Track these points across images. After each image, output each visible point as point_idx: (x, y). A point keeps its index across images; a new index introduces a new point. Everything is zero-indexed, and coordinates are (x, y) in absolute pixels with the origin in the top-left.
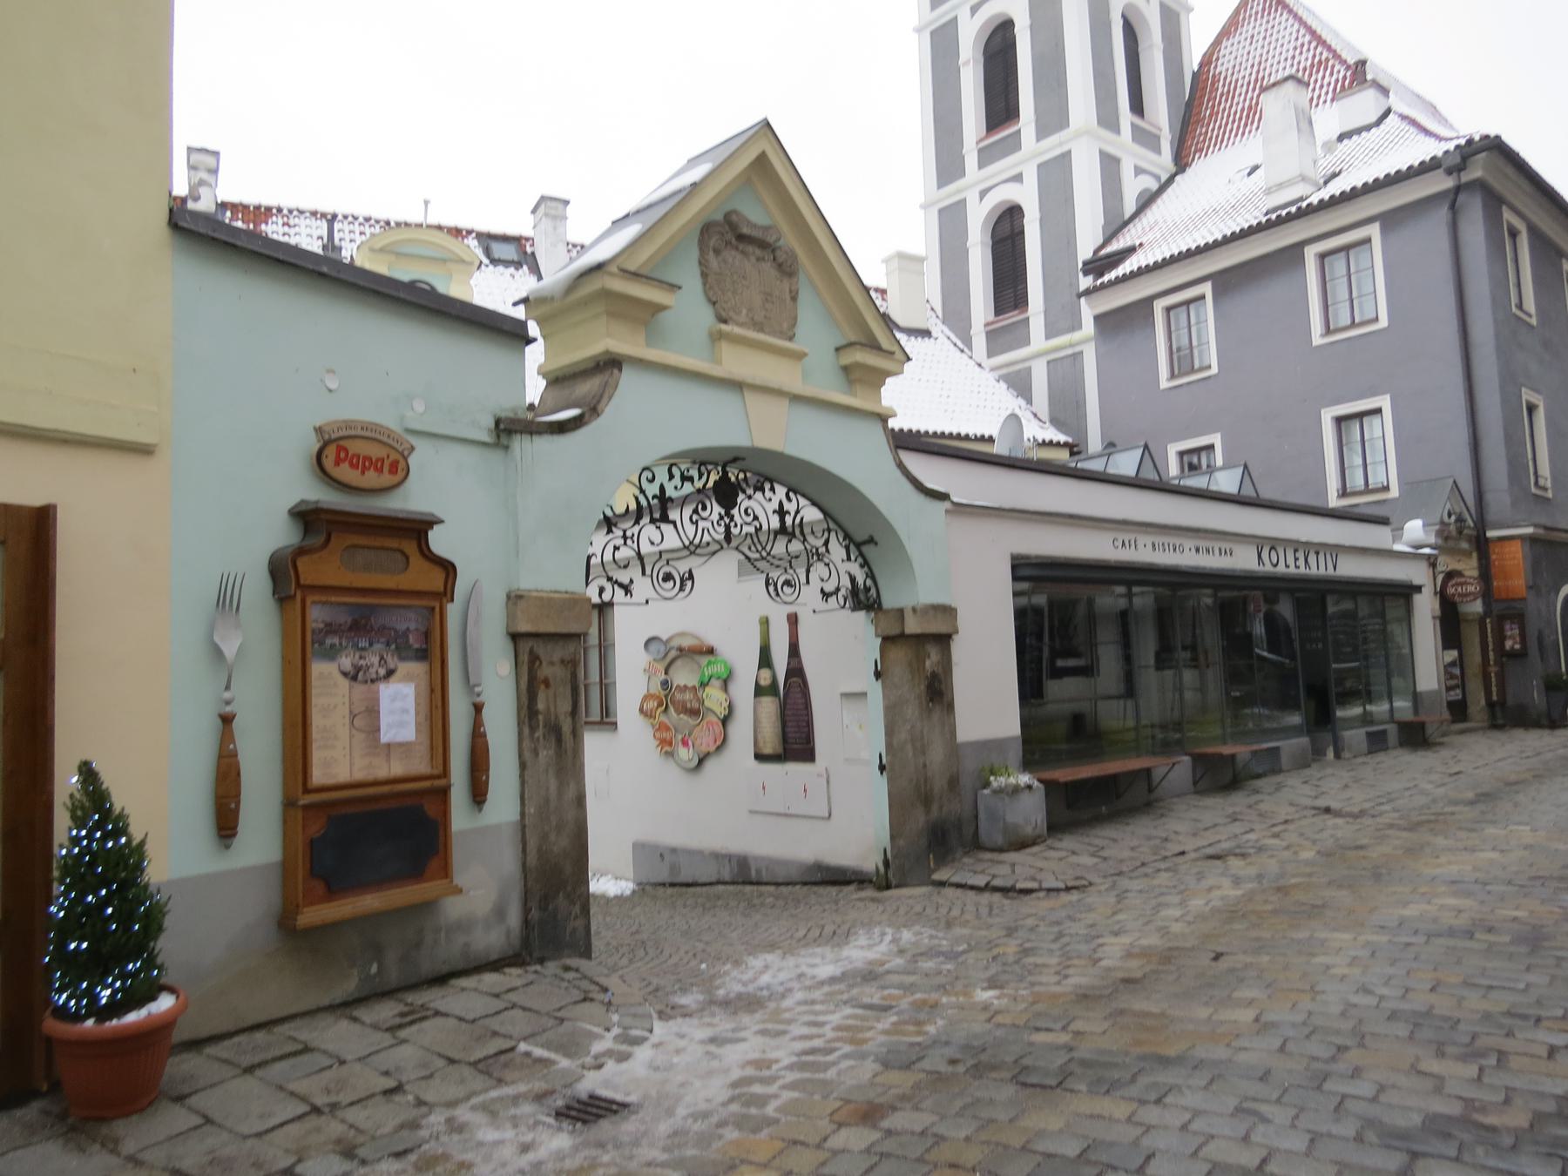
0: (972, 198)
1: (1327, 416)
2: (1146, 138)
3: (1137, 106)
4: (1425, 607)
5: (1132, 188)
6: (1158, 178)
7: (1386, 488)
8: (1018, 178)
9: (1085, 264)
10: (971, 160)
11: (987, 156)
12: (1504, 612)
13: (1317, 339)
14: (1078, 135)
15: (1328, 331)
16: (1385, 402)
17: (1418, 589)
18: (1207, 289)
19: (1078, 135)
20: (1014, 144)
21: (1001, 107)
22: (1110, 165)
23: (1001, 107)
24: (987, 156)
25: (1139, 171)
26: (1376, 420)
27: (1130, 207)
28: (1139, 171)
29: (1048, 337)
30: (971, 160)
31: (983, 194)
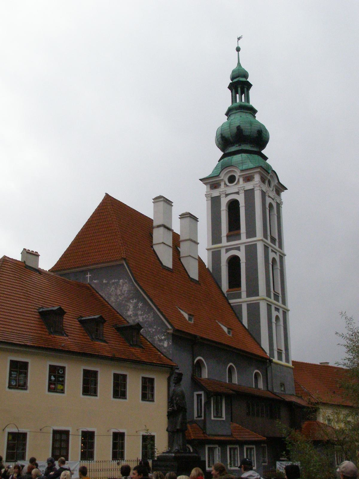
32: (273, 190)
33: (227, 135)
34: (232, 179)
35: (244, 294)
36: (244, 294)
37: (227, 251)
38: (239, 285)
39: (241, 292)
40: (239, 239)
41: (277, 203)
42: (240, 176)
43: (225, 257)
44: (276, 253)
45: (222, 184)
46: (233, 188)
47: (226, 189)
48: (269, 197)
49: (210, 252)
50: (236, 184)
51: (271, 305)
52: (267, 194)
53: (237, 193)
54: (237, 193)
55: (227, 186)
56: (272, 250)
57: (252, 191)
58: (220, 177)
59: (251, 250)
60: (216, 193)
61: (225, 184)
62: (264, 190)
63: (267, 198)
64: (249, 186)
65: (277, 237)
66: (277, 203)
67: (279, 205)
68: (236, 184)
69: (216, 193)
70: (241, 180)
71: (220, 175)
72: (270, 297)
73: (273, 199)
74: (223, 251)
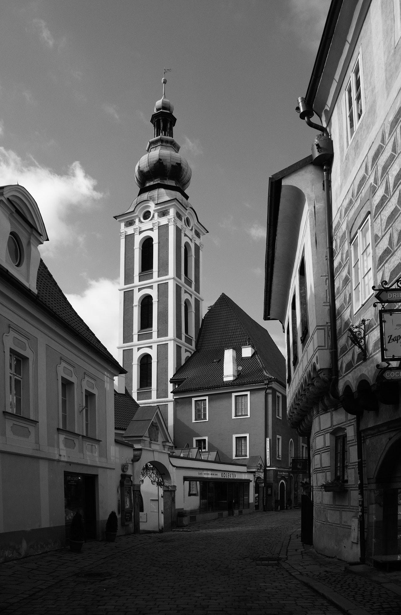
0: (135, 349)
1: (234, 436)
4: (252, 485)
5: (184, 355)
7: (246, 456)
8: (151, 347)
9: (171, 379)
10: (135, 337)
11: (140, 338)
12: (268, 485)
13: (234, 417)
15: (236, 416)
16: (247, 435)
17: (251, 481)
18: (207, 398)
19: (171, 340)
20: (150, 336)
21: (146, 322)
22: (178, 349)
23: (146, 322)
24: (140, 338)
25: (186, 351)
28: (186, 351)
30: (135, 337)
31: (139, 349)
33: (146, 170)
34: (147, 215)
35: (155, 334)
36: (155, 334)
37: (140, 290)
38: (150, 325)
40: (152, 278)
42: (154, 211)
43: (137, 297)
45: (137, 220)
46: (147, 224)
47: (141, 225)
48: (186, 235)
49: (123, 292)
50: (151, 220)
51: (181, 347)
52: (183, 231)
53: (152, 229)
54: (152, 229)
55: (142, 222)
57: (167, 226)
59: (163, 289)
60: (130, 230)
61: (140, 221)
62: (180, 227)
63: (183, 235)
68: (151, 220)
69: (130, 230)
71: (135, 211)
72: (181, 338)
74: (136, 290)
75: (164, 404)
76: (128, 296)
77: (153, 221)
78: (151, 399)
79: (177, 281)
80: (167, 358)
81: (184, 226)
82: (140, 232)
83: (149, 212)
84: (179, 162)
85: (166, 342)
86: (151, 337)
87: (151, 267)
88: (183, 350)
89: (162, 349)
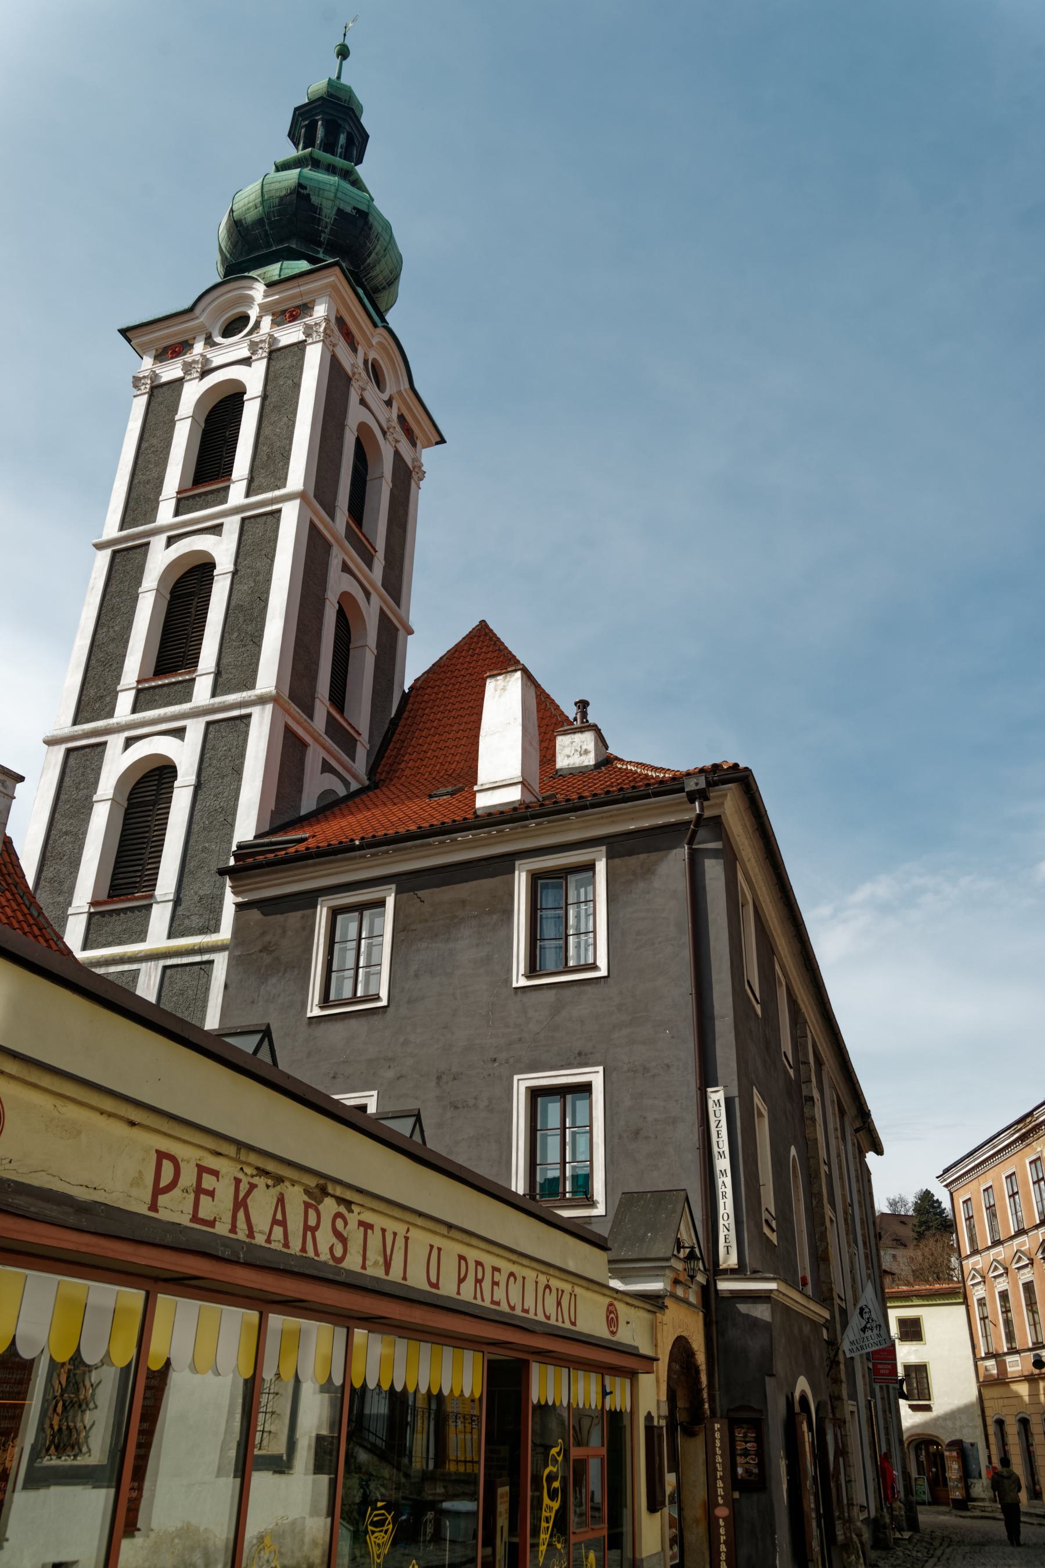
1: (522, 1084)
2: (341, 735)
3: (338, 697)
5: (315, 785)
6: (346, 784)
8: (179, 733)
9: (240, 847)
10: (125, 701)
14: (262, 700)
16: (596, 1077)
19: (262, 700)
21: (174, 650)
25: (326, 768)
26: (581, 1105)
27: (308, 804)
28: (326, 768)
29: (170, 936)
30: (125, 701)
31: (129, 742)
32: (389, 403)
33: (251, 216)
34: (235, 325)
39: (194, 680)
41: (397, 454)
44: (368, 595)
53: (246, 362)
55: (215, 344)
56: (344, 563)
58: (197, 318)
60: (171, 371)
64: (290, 335)
65: (380, 544)
66: (397, 454)
67: (406, 476)
69: (171, 371)
70: (266, 322)
71: (198, 310)
73: (384, 433)
75: (197, 959)
76: (126, 562)
77: (255, 337)
78: (143, 940)
79: (316, 513)
80: (238, 771)
81: (364, 374)
82: (204, 374)
83: (245, 319)
84: (364, 208)
85: (244, 711)
86: (188, 697)
87: (225, 471)
88: (314, 756)
89: (224, 738)
